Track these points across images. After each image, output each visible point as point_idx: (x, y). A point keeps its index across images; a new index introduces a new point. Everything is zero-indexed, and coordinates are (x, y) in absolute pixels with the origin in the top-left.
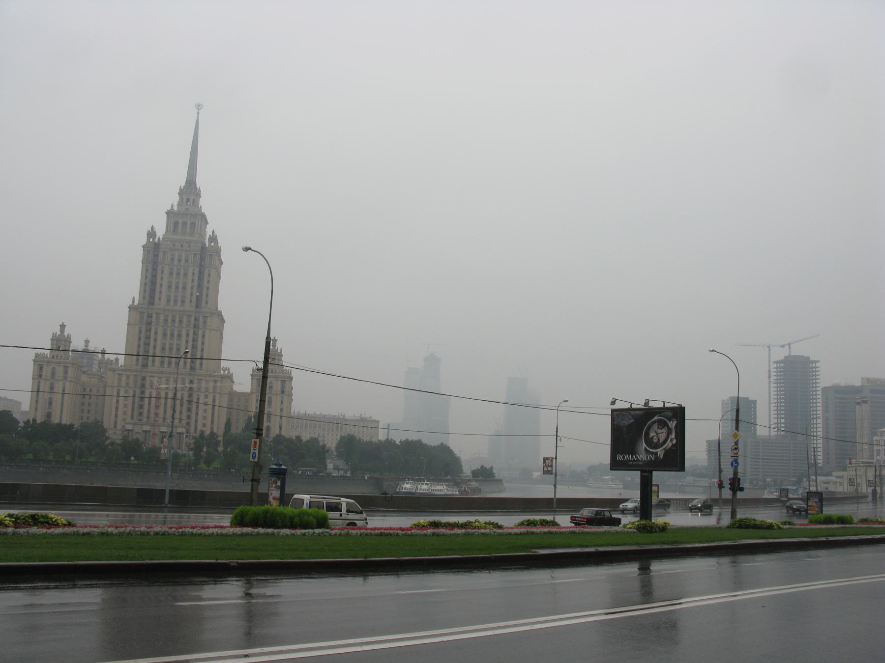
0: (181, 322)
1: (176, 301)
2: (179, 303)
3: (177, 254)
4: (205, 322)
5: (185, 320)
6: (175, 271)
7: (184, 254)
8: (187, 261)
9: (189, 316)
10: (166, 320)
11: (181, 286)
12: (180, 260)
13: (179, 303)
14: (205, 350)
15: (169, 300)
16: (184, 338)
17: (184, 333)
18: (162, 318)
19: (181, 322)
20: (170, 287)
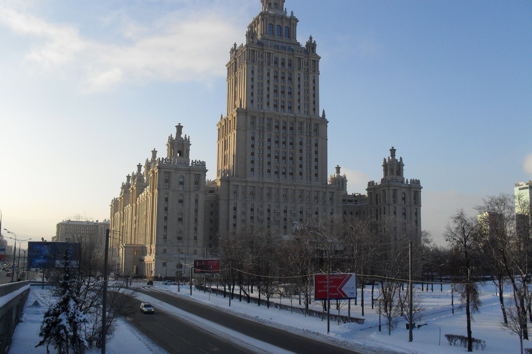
1: (283, 107)
2: (287, 109)
3: (280, 56)
4: (316, 130)
5: (297, 125)
6: (280, 76)
7: (287, 58)
8: (290, 65)
9: (301, 123)
11: (287, 91)
12: (283, 64)
13: (287, 109)
14: (319, 160)
15: (276, 106)
16: (298, 147)
17: (297, 141)
18: (274, 124)
20: (276, 91)
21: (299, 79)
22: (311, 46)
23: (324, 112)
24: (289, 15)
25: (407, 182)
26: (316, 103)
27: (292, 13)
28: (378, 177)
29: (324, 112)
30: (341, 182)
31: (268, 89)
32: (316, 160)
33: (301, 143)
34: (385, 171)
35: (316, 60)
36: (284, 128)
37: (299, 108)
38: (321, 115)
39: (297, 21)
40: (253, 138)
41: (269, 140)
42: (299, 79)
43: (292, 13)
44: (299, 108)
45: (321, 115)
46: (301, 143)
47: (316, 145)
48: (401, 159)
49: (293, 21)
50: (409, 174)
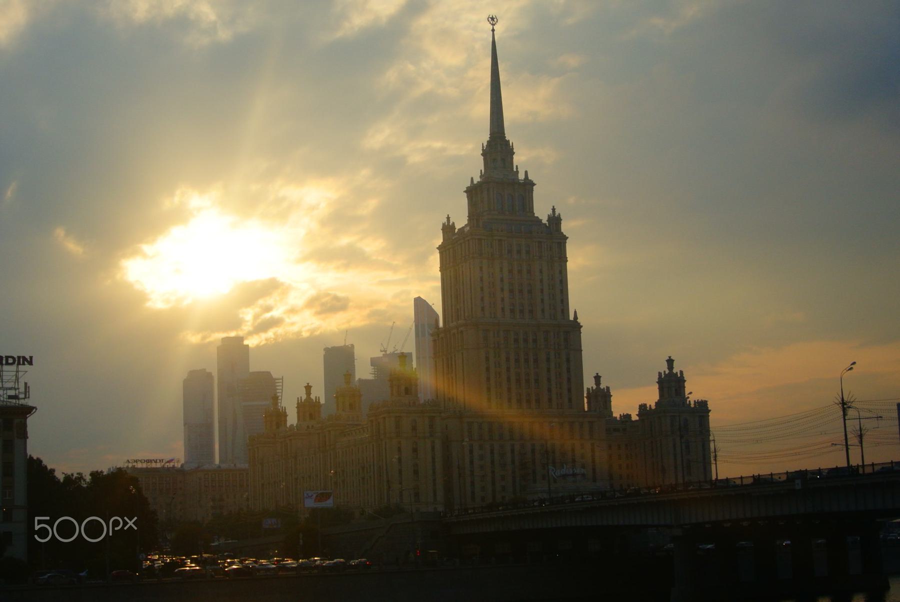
0: (535, 341)
8: (528, 252)
10: (516, 341)
19: (535, 341)
21: (541, 272)
22: (555, 220)
23: (575, 312)
24: (521, 176)
25: (690, 404)
26: (564, 301)
27: (526, 172)
28: (651, 396)
29: (575, 312)
30: (602, 397)
31: (502, 290)
32: (569, 380)
33: (548, 360)
34: (661, 389)
35: (562, 240)
36: (526, 341)
37: (543, 311)
38: (572, 318)
39: (532, 184)
40: (487, 359)
41: (508, 359)
42: (541, 272)
43: (526, 172)
44: (543, 311)
45: (572, 318)
46: (548, 360)
47: (568, 360)
48: (681, 372)
49: (528, 185)
50: (695, 391)
